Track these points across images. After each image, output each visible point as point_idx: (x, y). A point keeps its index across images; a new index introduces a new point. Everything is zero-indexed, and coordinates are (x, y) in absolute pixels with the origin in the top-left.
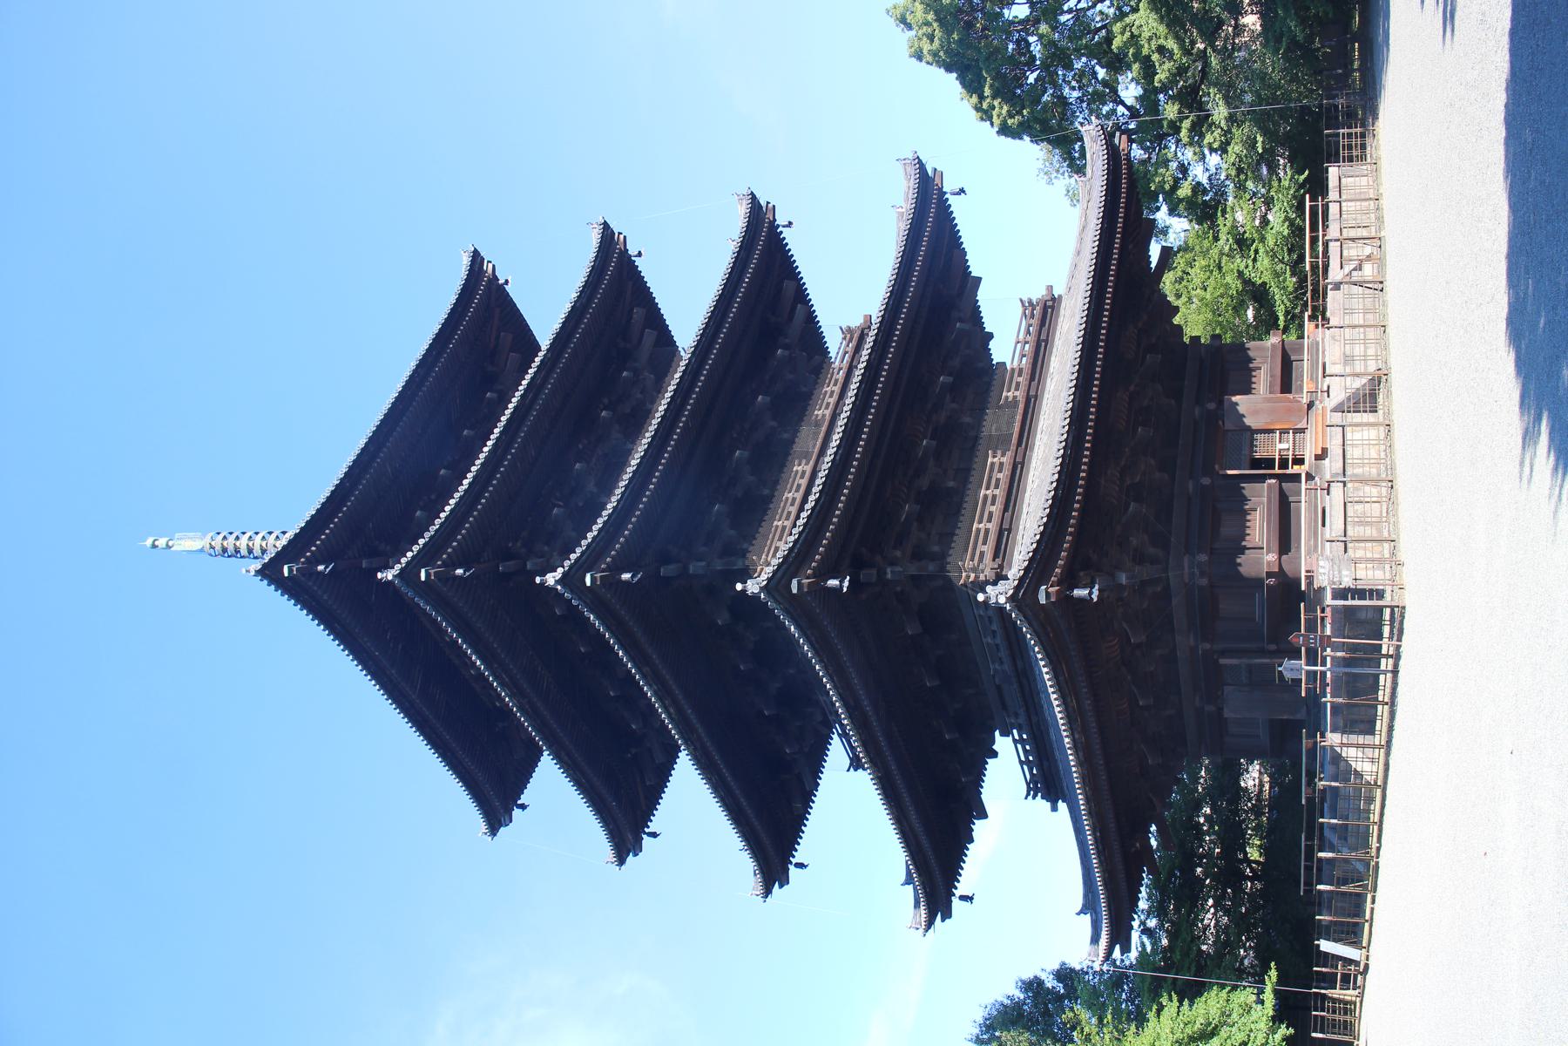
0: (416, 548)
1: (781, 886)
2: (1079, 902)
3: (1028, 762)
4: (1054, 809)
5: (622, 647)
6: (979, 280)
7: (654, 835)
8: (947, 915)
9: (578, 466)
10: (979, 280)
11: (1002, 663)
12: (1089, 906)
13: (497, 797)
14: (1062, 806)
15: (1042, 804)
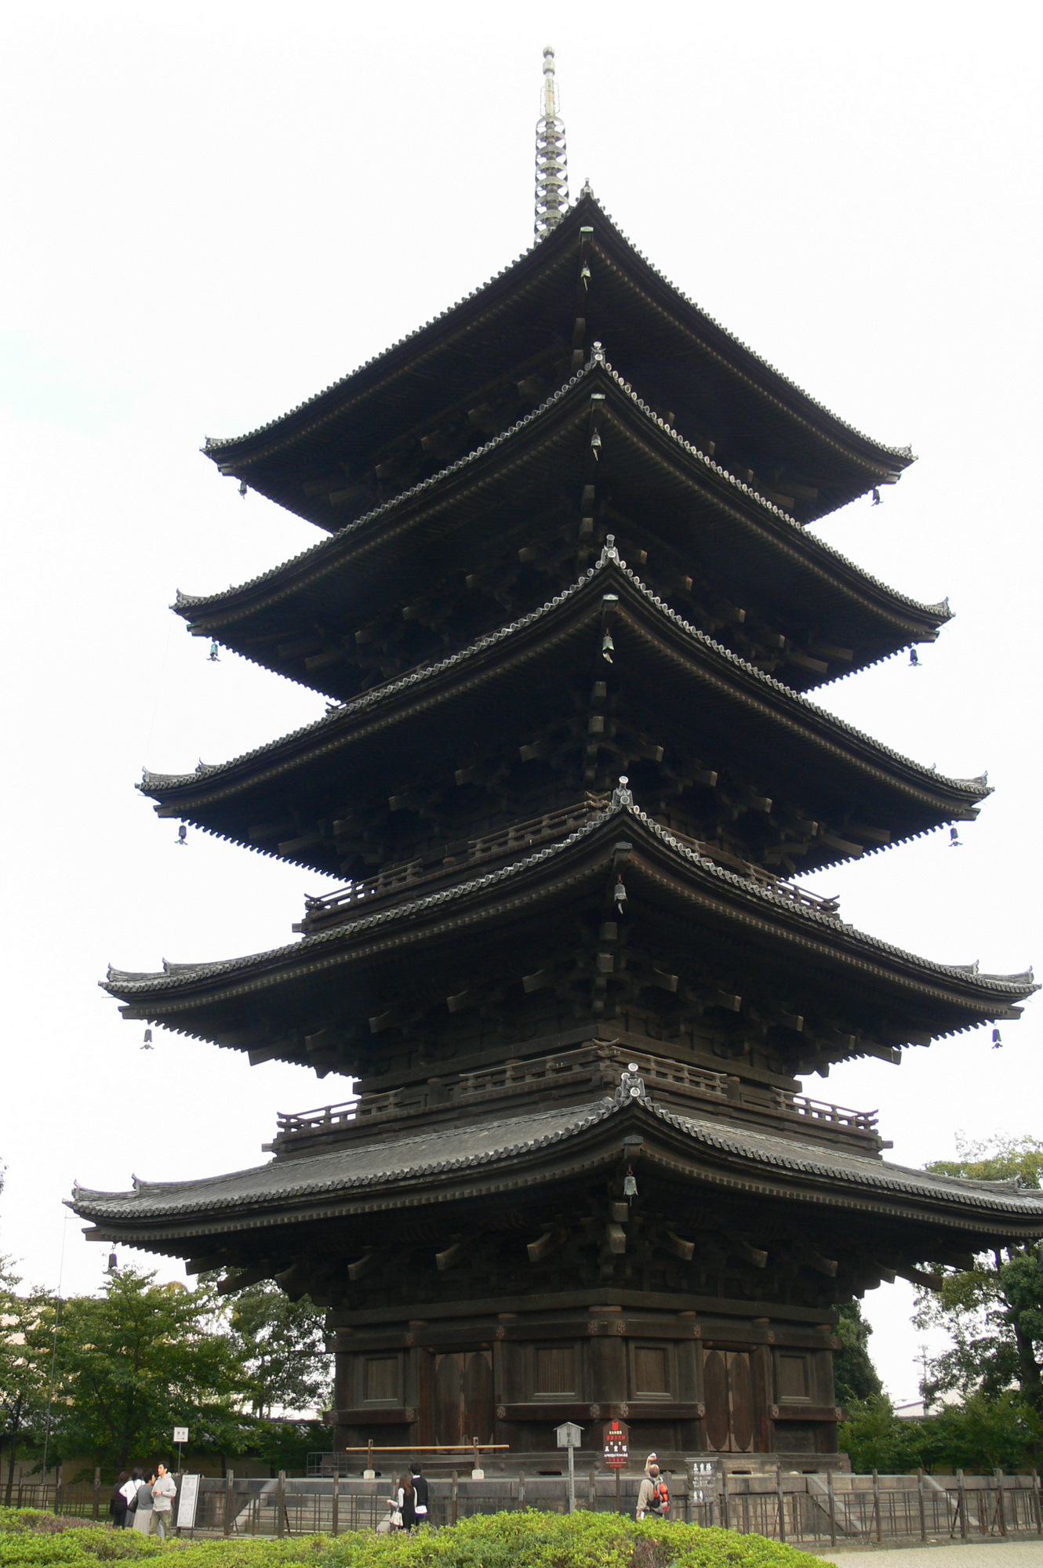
0: (627, 388)
1: (156, 809)
2: (151, 1177)
3: (328, 1117)
4: (265, 1148)
5: (516, 633)
6: (896, 1059)
7: (213, 656)
8: (127, 1013)
9: (690, 580)
10: (896, 1059)
11: (476, 1088)
12: (144, 1190)
13: (265, 461)
14: (271, 1156)
15: (271, 1132)
